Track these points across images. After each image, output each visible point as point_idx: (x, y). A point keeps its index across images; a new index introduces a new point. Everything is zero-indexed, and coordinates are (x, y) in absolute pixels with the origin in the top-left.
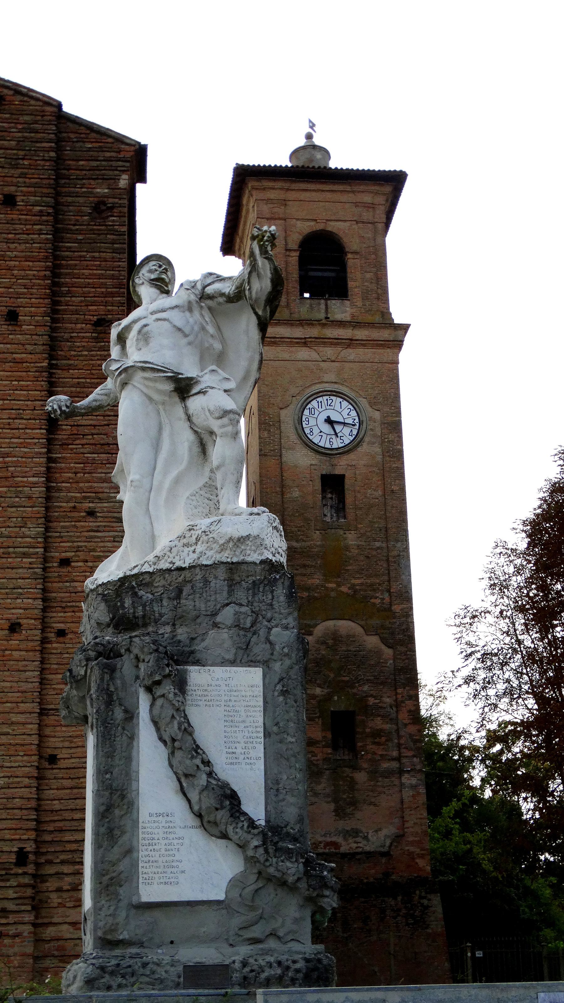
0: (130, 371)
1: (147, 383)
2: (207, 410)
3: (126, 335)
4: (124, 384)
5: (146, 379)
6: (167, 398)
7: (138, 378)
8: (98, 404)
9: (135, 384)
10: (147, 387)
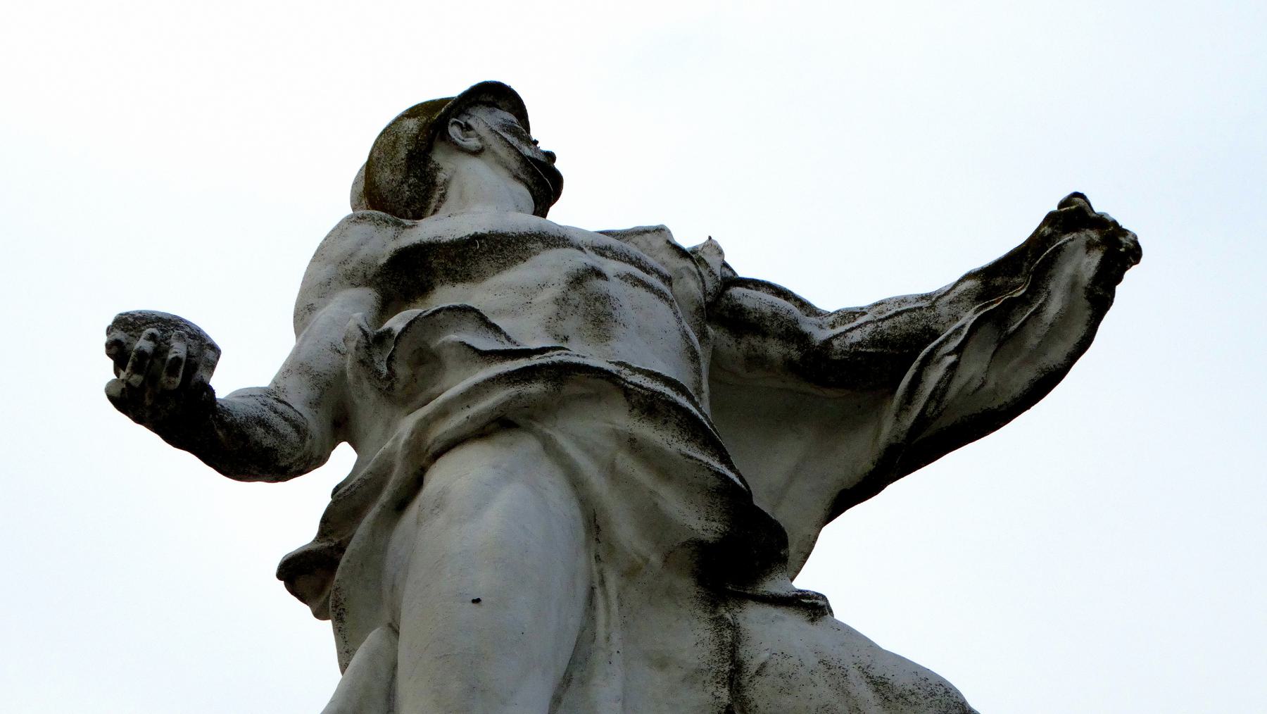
0: (569, 389)
1: (626, 463)
2: (854, 673)
3: (484, 265)
4: (499, 425)
5: (633, 445)
6: (655, 559)
7: (591, 430)
8: (269, 441)
9: (562, 441)
10: (612, 472)
